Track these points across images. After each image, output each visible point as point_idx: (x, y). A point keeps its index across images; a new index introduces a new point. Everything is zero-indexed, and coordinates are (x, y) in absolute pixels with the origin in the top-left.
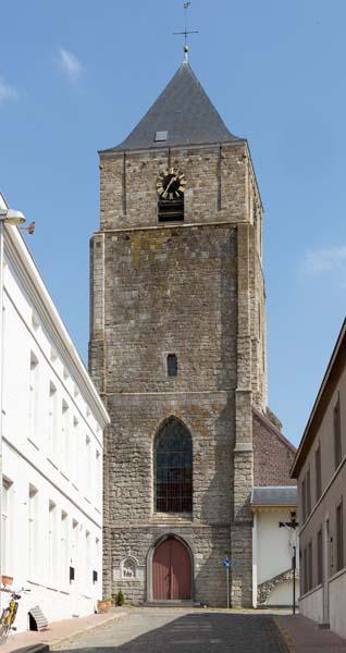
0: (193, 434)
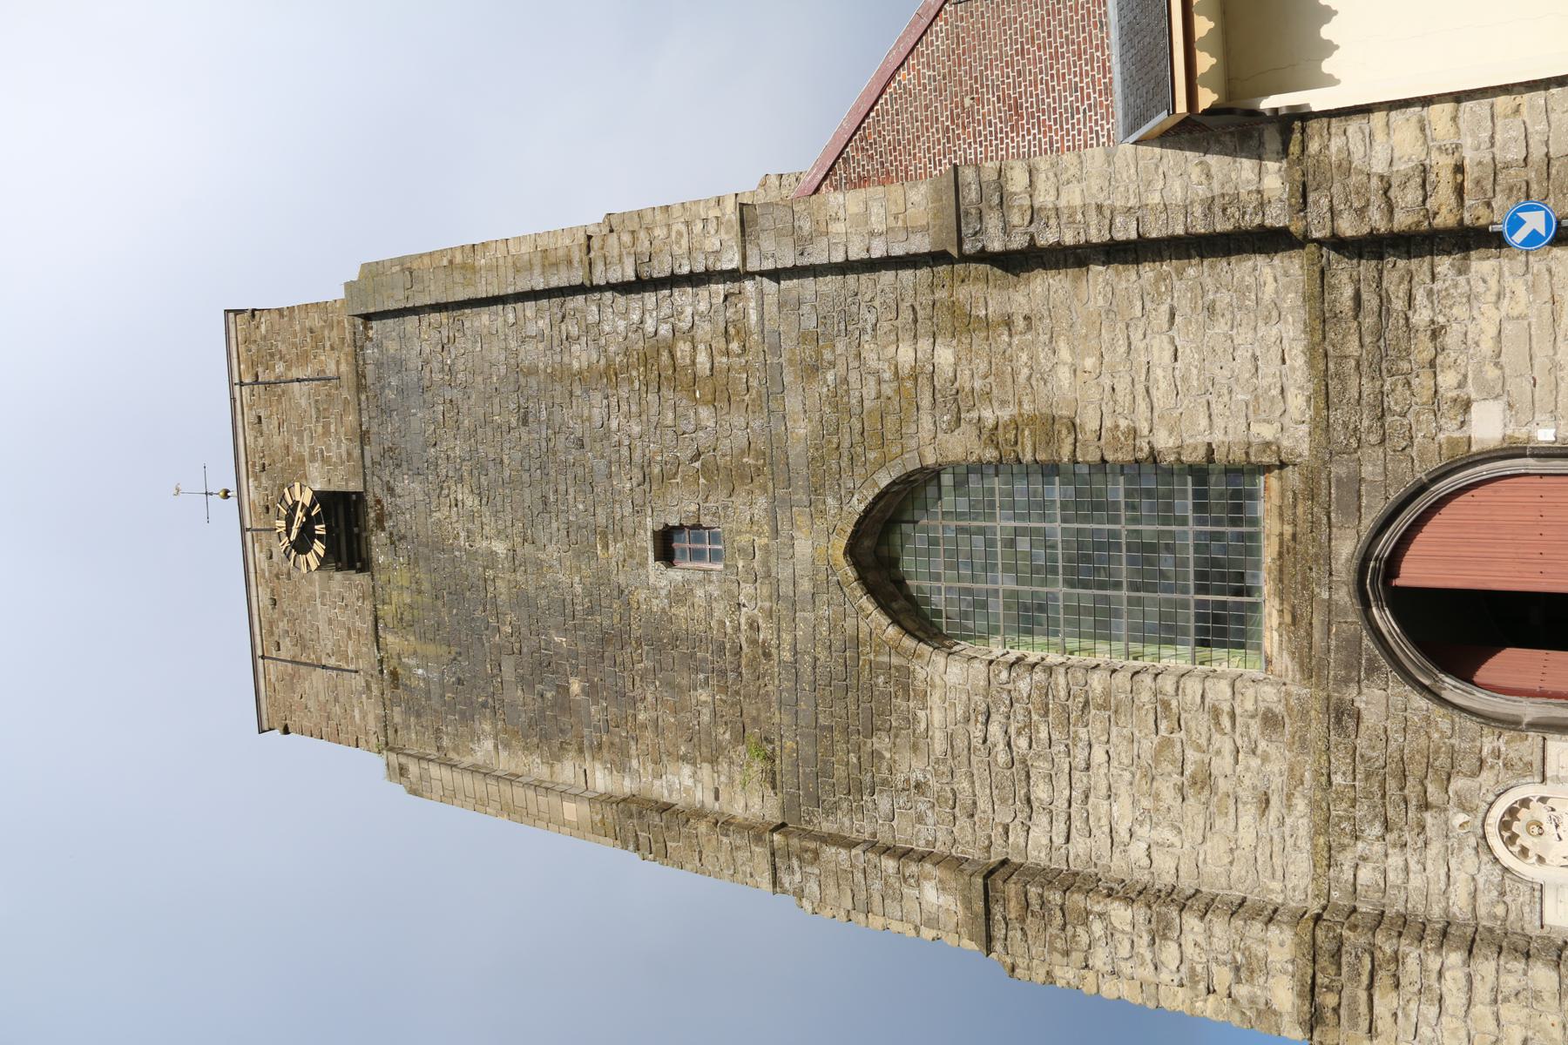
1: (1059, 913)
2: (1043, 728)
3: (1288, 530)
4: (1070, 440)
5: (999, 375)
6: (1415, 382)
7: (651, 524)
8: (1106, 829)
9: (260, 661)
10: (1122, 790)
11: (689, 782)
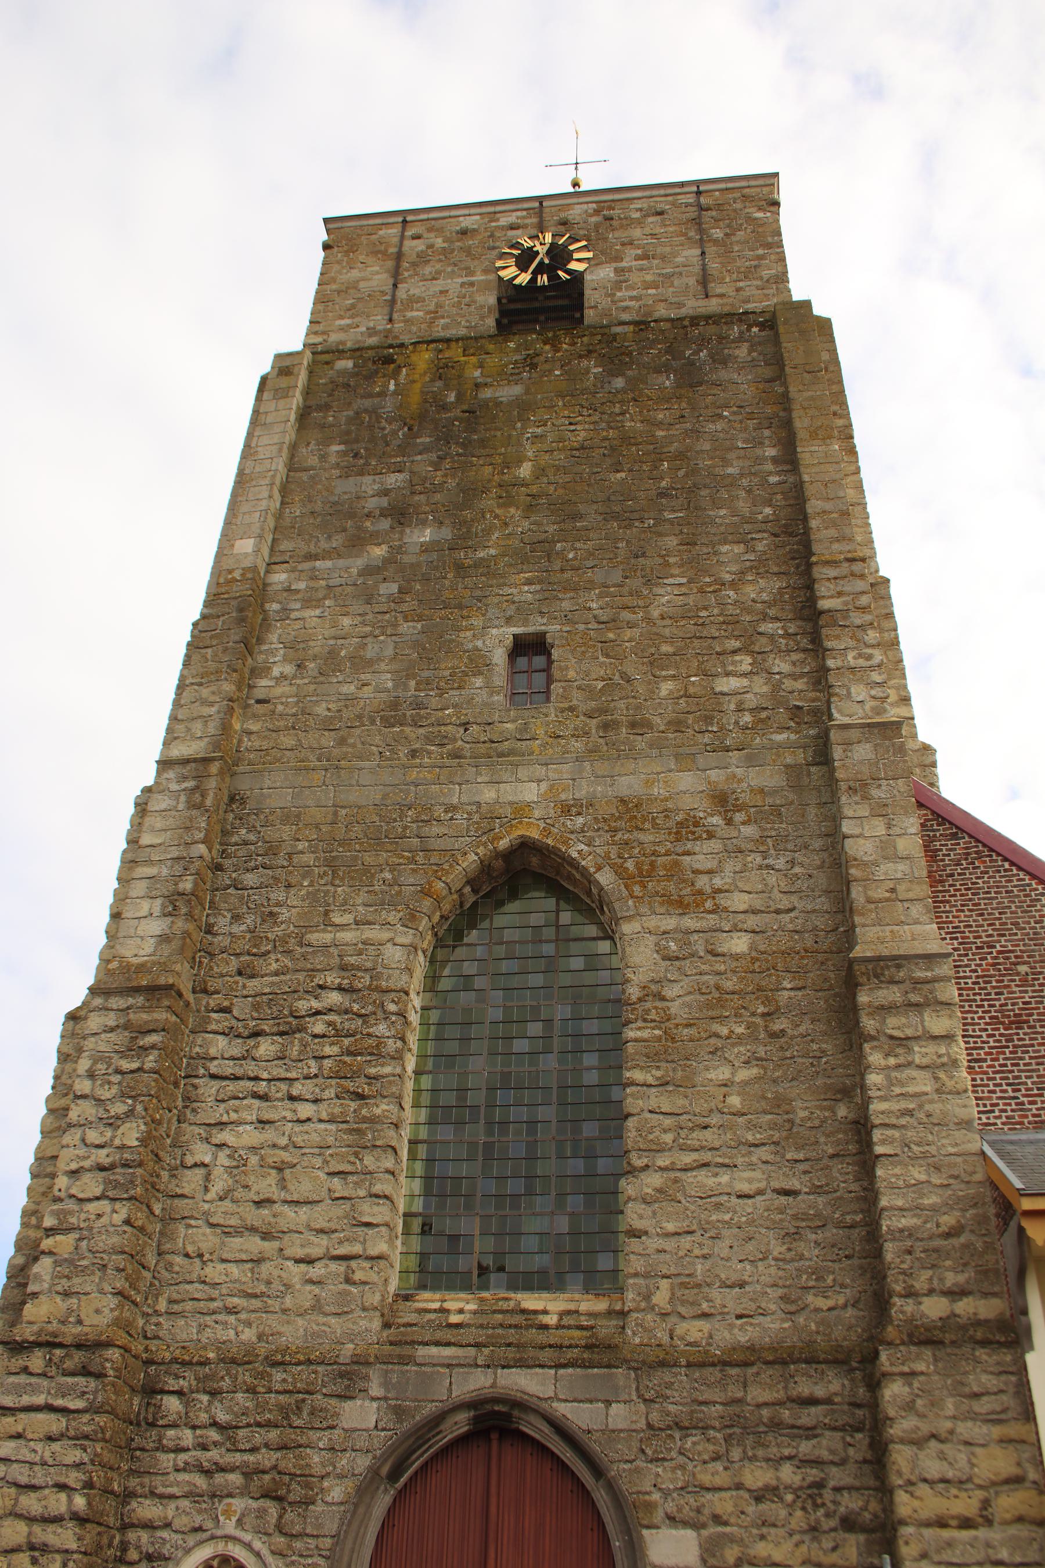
0: (625, 907)
1: (135, 1065)
2: (336, 1049)
3: (552, 1320)
4: (650, 1080)
5: (721, 1003)
6: (719, 1466)
7: (553, 629)
8: (225, 1118)
9: (400, 219)
10: (269, 1135)
11: (276, 671)
